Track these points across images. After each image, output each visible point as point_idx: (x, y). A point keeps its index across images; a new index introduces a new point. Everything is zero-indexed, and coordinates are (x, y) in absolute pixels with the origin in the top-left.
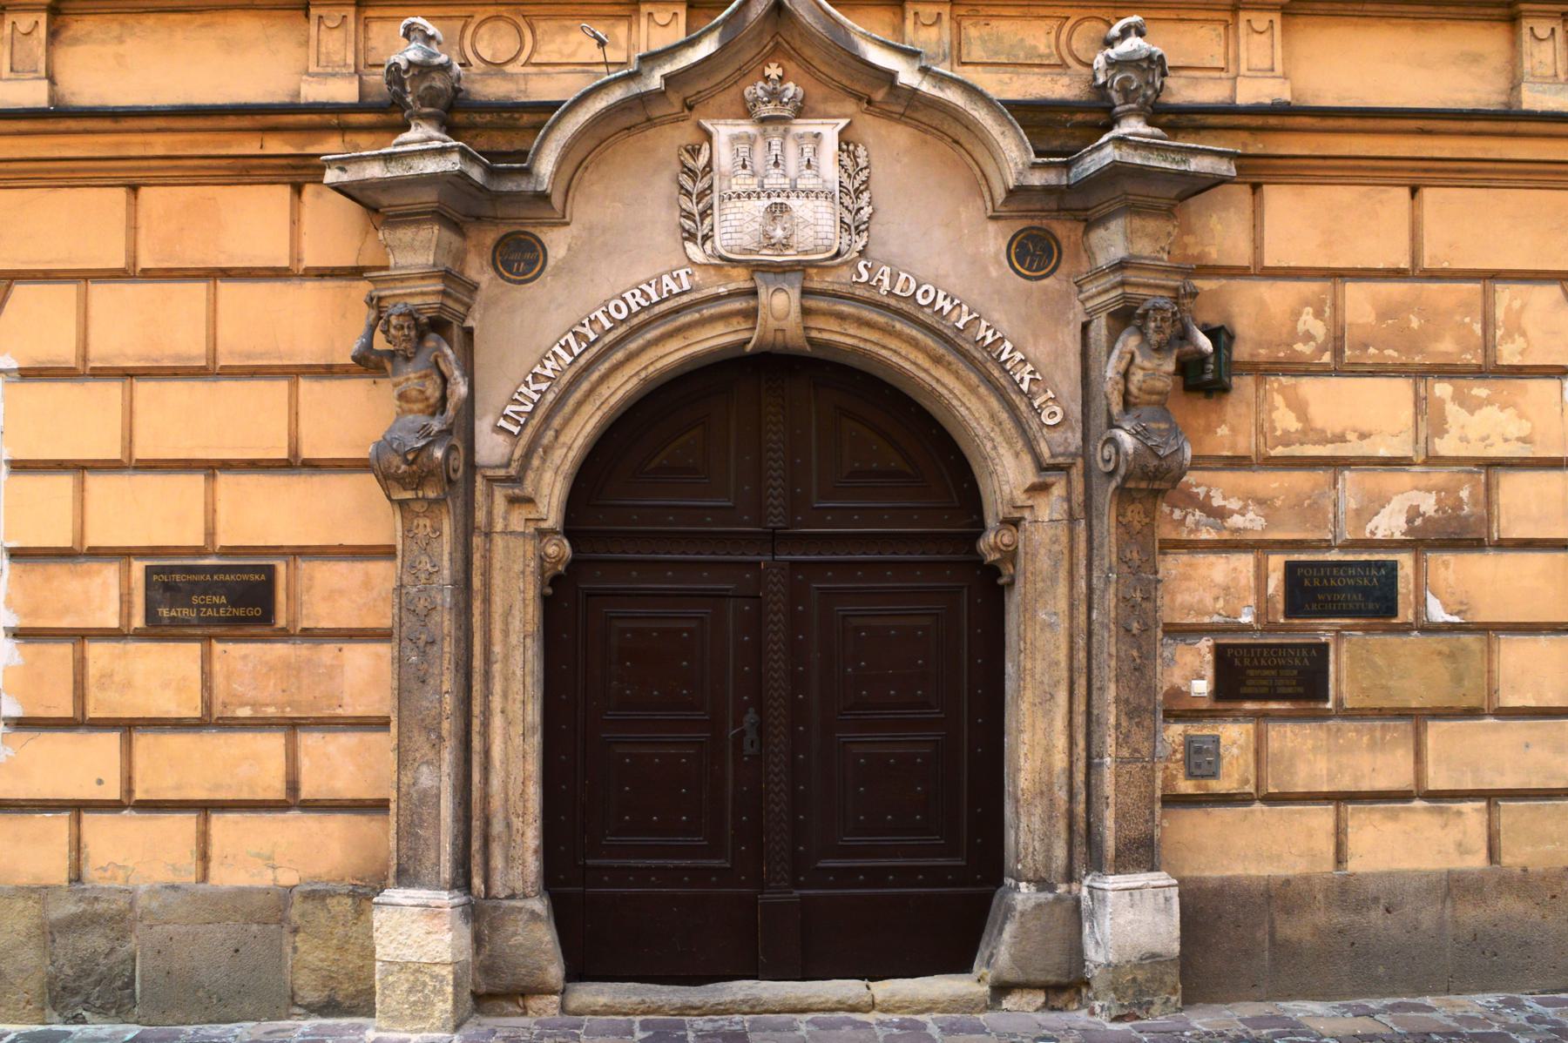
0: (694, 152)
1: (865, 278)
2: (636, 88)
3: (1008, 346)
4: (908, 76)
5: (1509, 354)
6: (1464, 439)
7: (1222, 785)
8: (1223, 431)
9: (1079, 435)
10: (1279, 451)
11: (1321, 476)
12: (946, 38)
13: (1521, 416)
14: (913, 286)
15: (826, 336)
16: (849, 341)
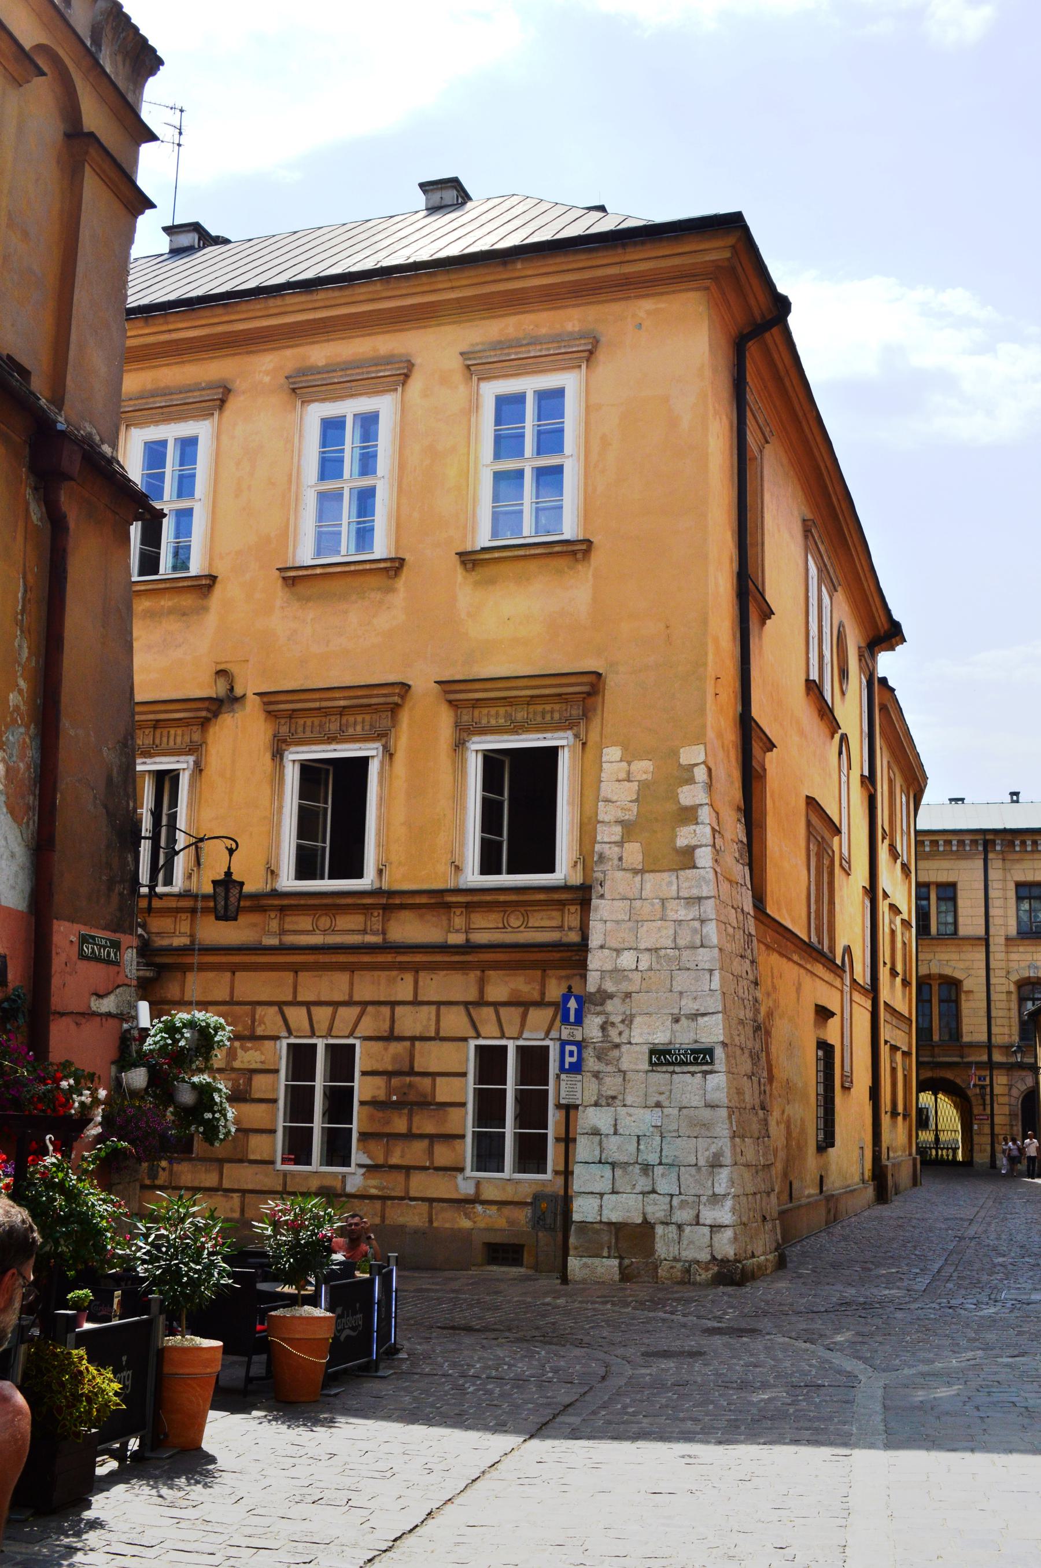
5: (259, 1031)
6: (242, 1062)
13: (262, 1053)
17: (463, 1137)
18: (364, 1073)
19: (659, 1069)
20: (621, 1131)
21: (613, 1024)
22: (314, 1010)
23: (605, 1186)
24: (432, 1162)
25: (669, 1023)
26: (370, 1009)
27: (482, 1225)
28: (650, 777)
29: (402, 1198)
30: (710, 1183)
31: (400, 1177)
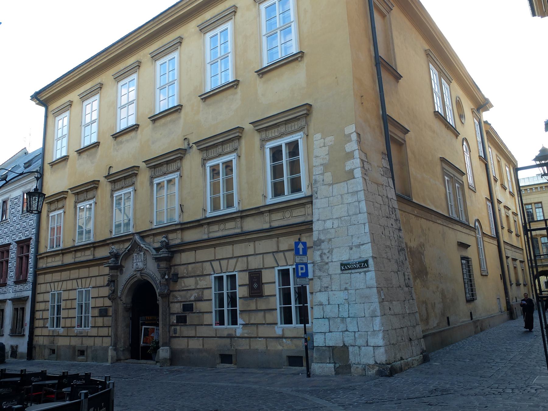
7: (177, 335)
17: (276, 309)
18: (240, 286)
19: (345, 272)
20: (331, 303)
21: (325, 254)
22: (221, 261)
23: (325, 329)
24: (265, 321)
25: (348, 250)
26: (240, 259)
27: (286, 348)
28: (333, 143)
29: (256, 338)
30: (371, 325)
31: (254, 328)
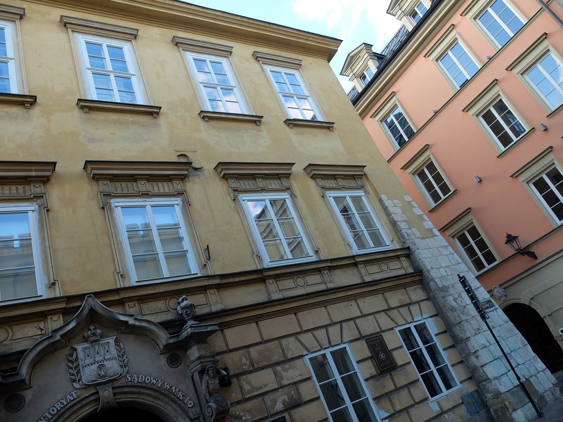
0: (71, 355)
1: (130, 379)
2: (52, 340)
3: (174, 388)
4: (131, 321)
5: (290, 356)
6: (288, 379)
8: (233, 395)
9: (199, 408)
10: (248, 396)
11: (260, 399)
12: (138, 309)
13: (297, 369)
14: (144, 378)
15: (121, 400)
16: (129, 399)
18: (358, 362)
